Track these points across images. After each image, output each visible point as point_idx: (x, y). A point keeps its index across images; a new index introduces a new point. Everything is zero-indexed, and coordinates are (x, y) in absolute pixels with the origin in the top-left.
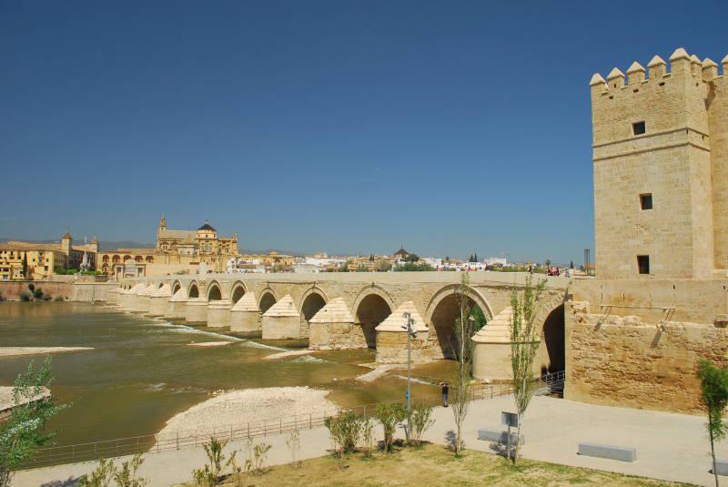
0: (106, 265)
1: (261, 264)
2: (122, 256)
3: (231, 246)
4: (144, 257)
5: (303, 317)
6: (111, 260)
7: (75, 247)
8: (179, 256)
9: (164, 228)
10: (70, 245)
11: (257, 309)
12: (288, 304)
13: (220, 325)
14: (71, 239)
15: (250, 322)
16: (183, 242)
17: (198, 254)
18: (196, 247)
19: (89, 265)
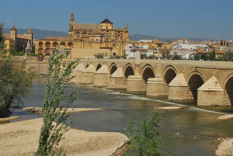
0: (41, 49)
1: (150, 48)
2: (52, 42)
3: (124, 35)
4: (67, 43)
5: (226, 91)
6: (44, 45)
7: (19, 36)
8: (90, 43)
9: (73, 21)
10: (16, 34)
11: (187, 85)
12: (215, 83)
13: (156, 95)
14: (16, 30)
15: (182, 94)
16: (93, 32)
17: (103, 41)
18: (102, 36)
19: (31, 49)
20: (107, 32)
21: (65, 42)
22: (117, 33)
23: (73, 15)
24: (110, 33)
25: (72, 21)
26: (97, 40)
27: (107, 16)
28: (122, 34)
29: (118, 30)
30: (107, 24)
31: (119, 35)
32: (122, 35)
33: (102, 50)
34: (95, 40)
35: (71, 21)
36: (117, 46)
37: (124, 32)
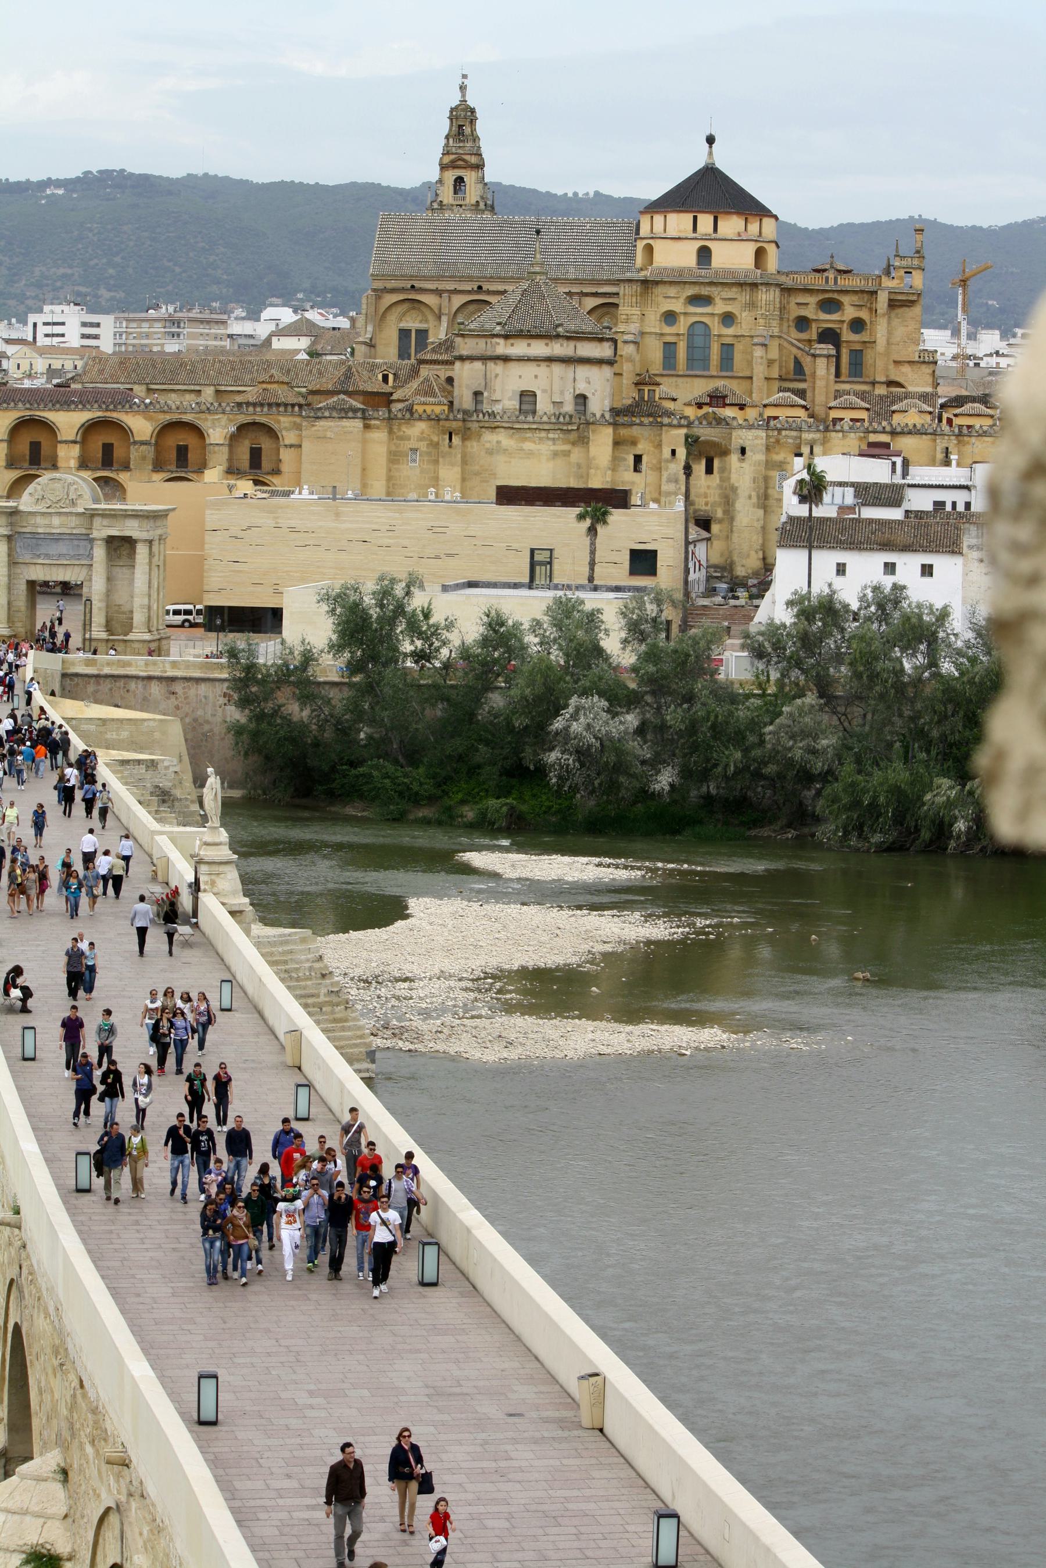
9: (470, 177)
20: (696, 300)
21: (206, 423)
22: (810, 313)
23: (473, 122)
24: (728, 319)
25: (460, 180)
26: (527, 397)
27: (710, 140)
28: (857, 325)
30: (705, 222)
31: (829, 336)
34: (511, 404)
35: (451, 176)
36: (734, 458)
37: (883, 298)
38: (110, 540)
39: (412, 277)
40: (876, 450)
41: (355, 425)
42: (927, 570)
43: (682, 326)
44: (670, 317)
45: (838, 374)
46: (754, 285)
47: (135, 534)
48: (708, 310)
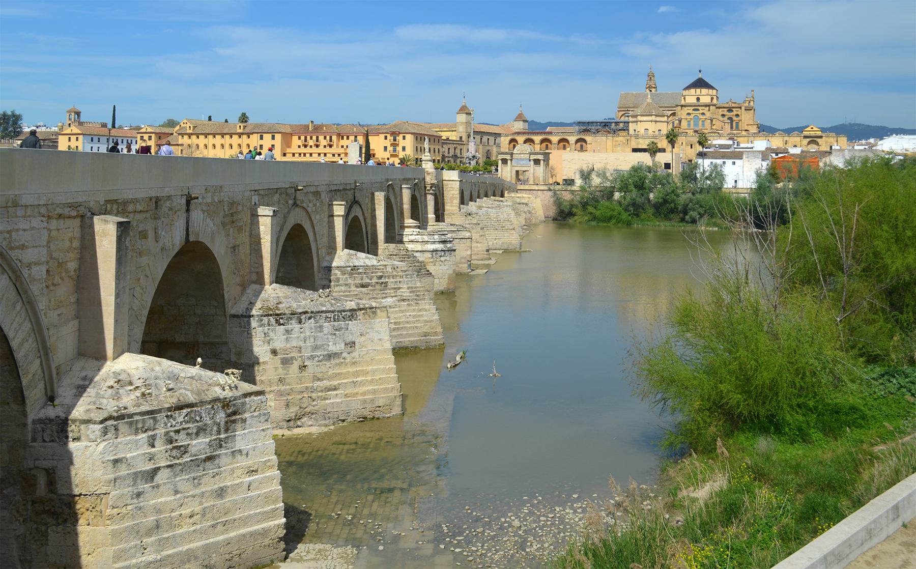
2: (537, 139)
21: (569, 138)
22: (726, 113)
24: (703, 114)
28: (737, 115)
29: (727, 105)
32: (739, 119)
33: (638, 154)
37: (743, 108)
38: (535, 160)
39: (627, 108)
40: (730, 139)
41: (604, 138)
42: (734, 163)
43: (693, 115)
44: (689, 114)
45: (732, 128)
46: (709, 106)
47: (540, 158)
48: (698, 112)
